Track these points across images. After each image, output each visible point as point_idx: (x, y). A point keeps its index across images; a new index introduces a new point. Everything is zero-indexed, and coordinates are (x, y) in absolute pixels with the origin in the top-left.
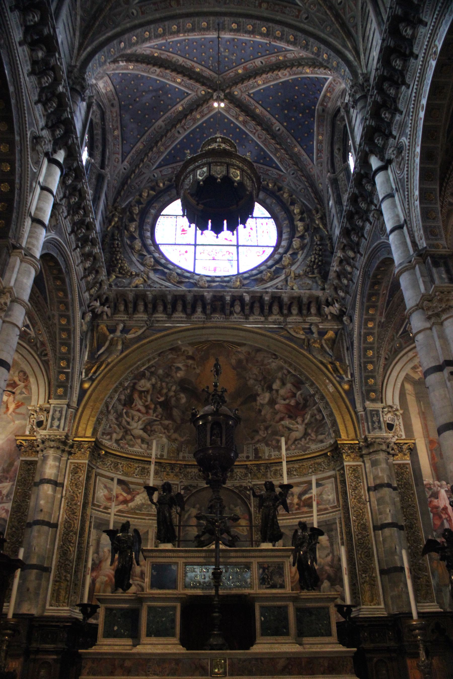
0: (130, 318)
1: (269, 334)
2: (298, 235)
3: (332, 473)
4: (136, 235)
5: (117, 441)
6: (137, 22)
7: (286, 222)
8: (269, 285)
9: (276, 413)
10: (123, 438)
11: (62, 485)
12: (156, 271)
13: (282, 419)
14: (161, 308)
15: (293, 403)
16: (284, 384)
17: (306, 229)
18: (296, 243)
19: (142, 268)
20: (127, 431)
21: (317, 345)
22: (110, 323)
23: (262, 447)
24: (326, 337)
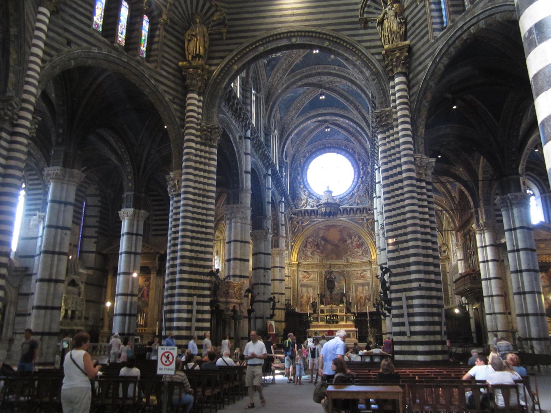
0: (303, 218)
1: (350, 221)
2: (361, 176)
3: (369, 268)
4: (301, 181)
5: (304, 259)
6: (296, 124)
7: (357, 169)
8: (350, 201)
9: (353, 246)
10: (305, 258)
11: (290, 276)
12: (310, 197)
13: (355, 248)
14: (313, 214)
15: (358, 243)
16: (355, 237)
17: (364, 173)
18: (359, 182)
19: (305, 197)
20: (306, 255)
21: (366, 225)
22: (296, 220)
23: (349, 257)
24: (369, 221)
